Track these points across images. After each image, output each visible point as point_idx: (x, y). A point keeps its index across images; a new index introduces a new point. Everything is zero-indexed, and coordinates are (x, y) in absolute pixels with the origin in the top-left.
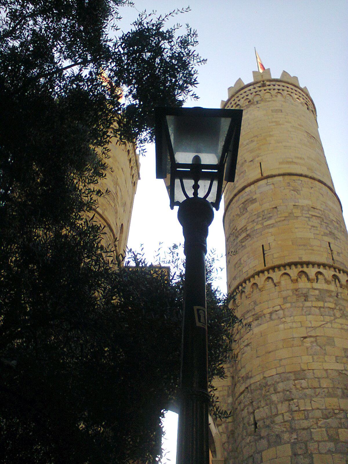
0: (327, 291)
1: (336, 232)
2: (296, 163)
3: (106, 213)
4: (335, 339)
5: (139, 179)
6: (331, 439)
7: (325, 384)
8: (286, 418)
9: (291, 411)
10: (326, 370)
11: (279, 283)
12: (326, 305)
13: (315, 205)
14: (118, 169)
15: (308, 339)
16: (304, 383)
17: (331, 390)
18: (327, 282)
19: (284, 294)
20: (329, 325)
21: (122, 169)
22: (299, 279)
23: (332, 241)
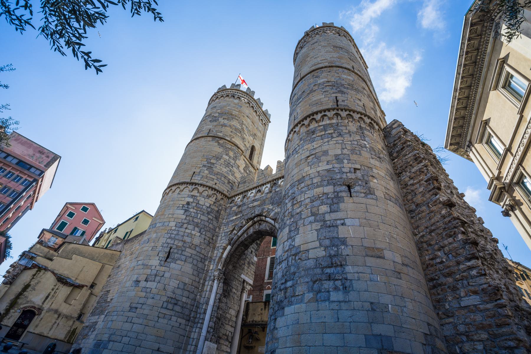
0: (329, 124)
1: (345, 90)
2: (321, 63)
3: (233, 139)
4: (329, 151)
5: (270, 122)
6: (313, 214)
7: (315, 181)
8: (290, 210)
9: (293, 205)
10: (318, 172)
11: (299, 131)
12: (327, 132)
13: (329, 80)
14: (244, 117)
15: (311, 157)
16: (303, 185)
17: (319, 183)
18: (330, 119)
19: (301, 137)
20: (326, 144)
21: (247, 116)
22: (311, 124)
23: (339, 95)
